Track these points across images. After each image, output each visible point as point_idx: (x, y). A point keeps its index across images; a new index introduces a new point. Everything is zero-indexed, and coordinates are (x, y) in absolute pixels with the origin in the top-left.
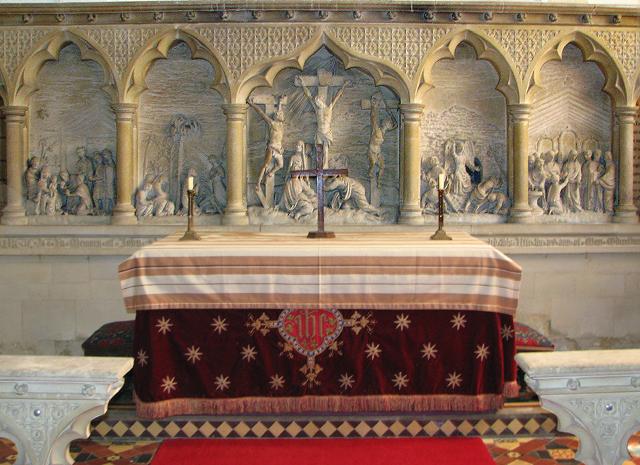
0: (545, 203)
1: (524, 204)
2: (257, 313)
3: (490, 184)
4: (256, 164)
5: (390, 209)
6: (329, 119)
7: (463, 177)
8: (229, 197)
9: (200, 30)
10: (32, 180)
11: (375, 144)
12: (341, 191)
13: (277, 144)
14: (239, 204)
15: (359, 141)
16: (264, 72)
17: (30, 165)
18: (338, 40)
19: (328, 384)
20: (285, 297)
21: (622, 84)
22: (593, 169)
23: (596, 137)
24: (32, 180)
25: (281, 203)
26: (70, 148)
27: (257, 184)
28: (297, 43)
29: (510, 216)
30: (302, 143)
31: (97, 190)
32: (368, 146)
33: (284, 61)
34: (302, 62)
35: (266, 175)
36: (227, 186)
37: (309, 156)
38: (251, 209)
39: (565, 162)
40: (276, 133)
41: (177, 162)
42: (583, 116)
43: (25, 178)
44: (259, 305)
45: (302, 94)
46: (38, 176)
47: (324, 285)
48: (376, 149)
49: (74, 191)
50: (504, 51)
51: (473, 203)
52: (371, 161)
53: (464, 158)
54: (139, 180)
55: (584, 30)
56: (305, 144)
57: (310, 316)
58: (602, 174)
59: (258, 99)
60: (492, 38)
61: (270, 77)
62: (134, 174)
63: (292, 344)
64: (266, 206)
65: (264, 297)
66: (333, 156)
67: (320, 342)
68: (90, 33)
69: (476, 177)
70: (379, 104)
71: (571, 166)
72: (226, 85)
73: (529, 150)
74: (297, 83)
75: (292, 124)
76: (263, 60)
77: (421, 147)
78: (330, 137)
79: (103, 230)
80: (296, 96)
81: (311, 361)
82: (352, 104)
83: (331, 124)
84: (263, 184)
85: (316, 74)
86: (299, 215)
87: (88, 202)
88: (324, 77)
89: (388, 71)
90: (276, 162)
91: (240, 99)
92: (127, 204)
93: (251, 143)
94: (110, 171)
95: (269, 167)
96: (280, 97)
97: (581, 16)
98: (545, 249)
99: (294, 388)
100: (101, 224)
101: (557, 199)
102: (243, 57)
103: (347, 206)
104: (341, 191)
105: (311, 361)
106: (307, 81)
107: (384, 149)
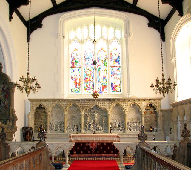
0: (130, 129)
1: (126, 130)
2: (86, 143)
3: (121, 127)
4: (85, 124)
7: (117, 125)
8: (81, 129)
9: (76, 102)
10: (51, 126)
12: (98, 128)
13: (88, 121)
14: (83, 130)
15: (101, 120)
16: (86, 109)
17: (50, 124)
19: (96, 153)
20: (90, 141)
21: (141, 110)
22: (138, 123)
23: (138, 118)
24: (51, 126)
26: (57, 121)
29: (124, 132)
31: (61, 128)
36: (81, 127)
37: (93, 122)
39: (133, 123)
41: (73, 123)
42: (136, 115)
43: (50, 125)
44: (87, 142)
46: (52, 125)
47: (95, 139)
49: (57, 128)
50: (123, 106)
51: (119, 130)
53: (117, 123)
54: (67, 127)
55: (135, 102)
57: (93, 143)
58: (139, 124)
59: (85, 113)
60: (120, 104)
61: (87, 110)
62: (67, 125)
63: (91, 147)
64: (87, 130)
65: (87, 141)
67: (94, 147)
68: (60, 103)
69: (119, 126)
71: (134, 124)
73: (127, 121)
77: (110, 120)
79: (62, 134)
81: (93, 149)
83: (96, 117)
87: (59, 129)
88: (96, 110)
91: (83, 114)
92: (66, 130)
94: (63, 125)
95: (87, 124)
97: (134, 100)
98: (129, 137)
99: (91, 153)
100: (61, 133)
101: (132, 128)
105: (93, 149)
106: (93, 111)
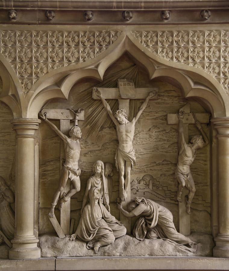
5: (202, 238)
6: (131, 135)
11: (184, 164)
13: (74, 165)
16: (59, 83)
18: (142, 46)
25: (78, 232)
27: (50, 209)
28: (97, 50)
30: (101, 163)
32: (176, 165)
33: (82, 69)
34: (101, 71)
35: (61, 199)
37: (109, 177)
38: (43, 239)
40: (72, 152)
45: (100, 108)
48: (185, 169)
52: (179, 183)
56: (105, 164)
59: (52, 114)
61: (65, 88)
64: (61, 235)
66: (135, 177)
70: (188, 119)
72: (15, 97)
74: (95, 96)
75: (90, 142)
76: (59, 69)
78: (133, 156)
80: (93, 112)
82: (155, 119)
84: (58, 210)
85: (116, 86)
86: (98, 245)
89: (199, 80)
90: (72, 184)
93: (43, 163)
95: (64, 190)
96: (76, 112)
102: (35, 65)
103: (154, 235)
104: (147, 217)
107: (192, 168)
